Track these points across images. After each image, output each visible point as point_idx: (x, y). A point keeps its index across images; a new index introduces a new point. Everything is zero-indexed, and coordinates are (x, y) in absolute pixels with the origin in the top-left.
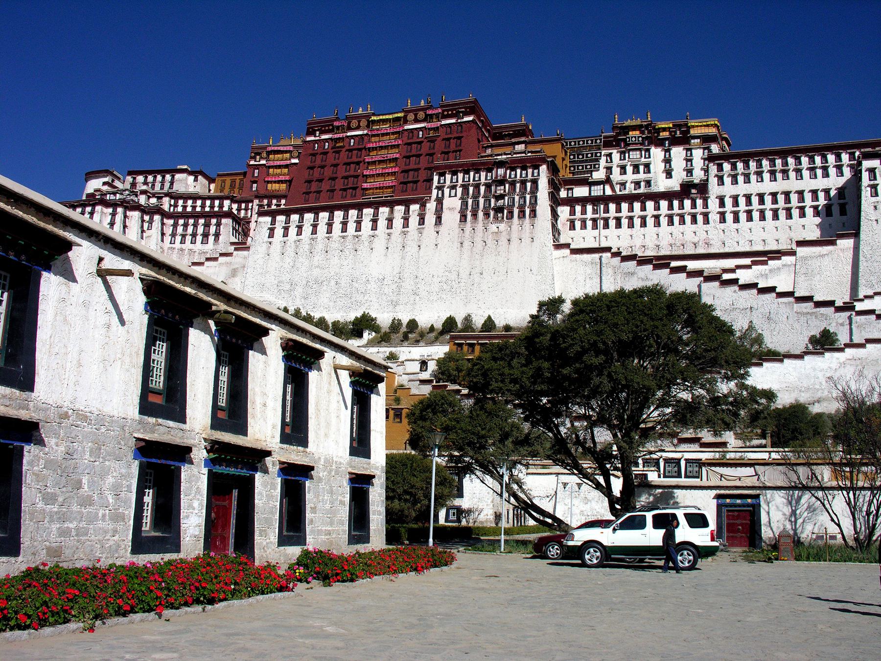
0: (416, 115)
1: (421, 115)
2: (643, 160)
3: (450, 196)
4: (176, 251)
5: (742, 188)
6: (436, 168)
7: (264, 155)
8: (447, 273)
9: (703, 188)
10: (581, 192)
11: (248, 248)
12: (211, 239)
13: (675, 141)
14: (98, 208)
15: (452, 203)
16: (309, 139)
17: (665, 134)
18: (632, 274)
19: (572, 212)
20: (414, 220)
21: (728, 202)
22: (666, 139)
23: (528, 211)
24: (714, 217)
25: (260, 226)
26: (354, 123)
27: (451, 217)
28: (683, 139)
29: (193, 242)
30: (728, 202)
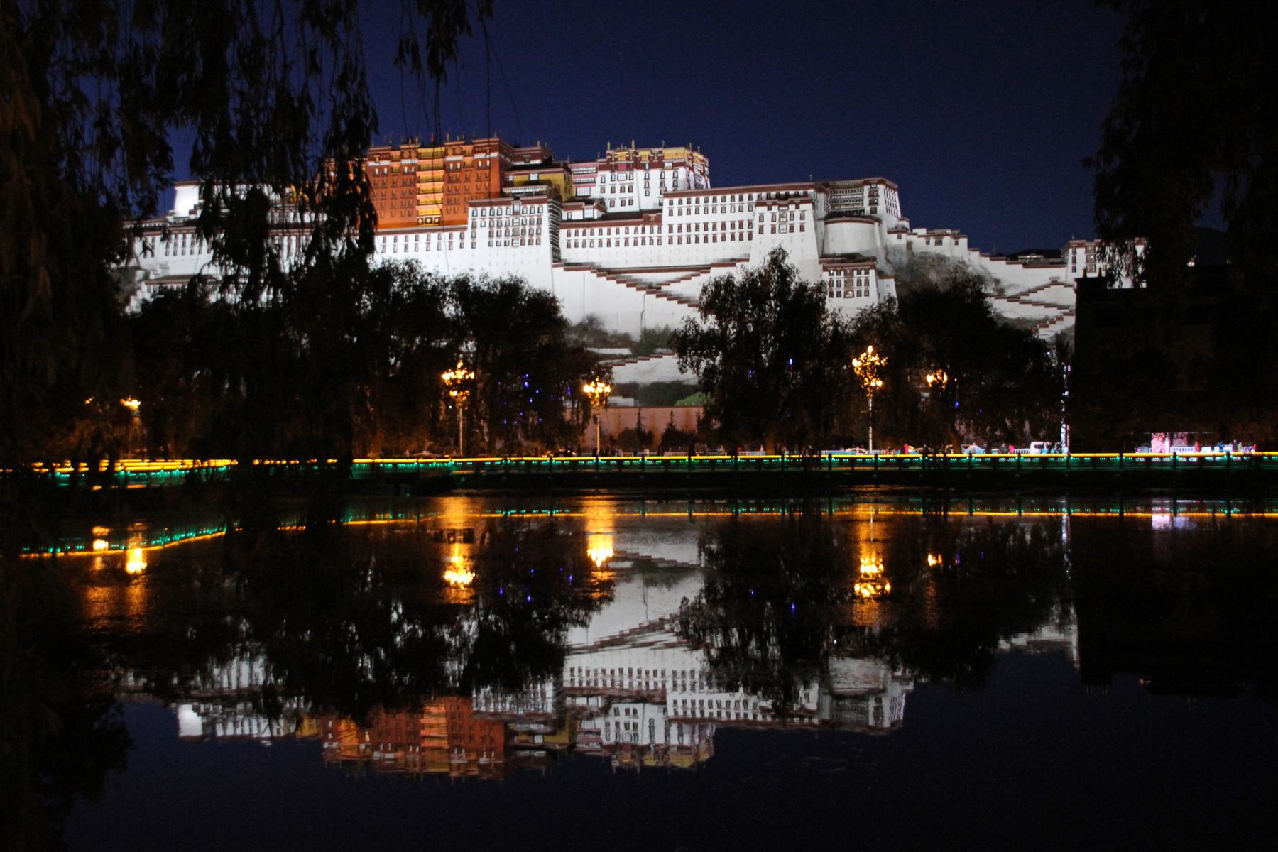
1: (458, 151)
5: (685, 219)
6: (473, 205)
9: (659, 221)
10: (577, 215)
13: (653, 166)
15: (482, 233)
17: (645, 161)
19: (569, 235)
21: (675, 229)
23: (535, 238)
24: (665, 240)
26: (406, 154)
28: (658, 164)
30: (675, 229)
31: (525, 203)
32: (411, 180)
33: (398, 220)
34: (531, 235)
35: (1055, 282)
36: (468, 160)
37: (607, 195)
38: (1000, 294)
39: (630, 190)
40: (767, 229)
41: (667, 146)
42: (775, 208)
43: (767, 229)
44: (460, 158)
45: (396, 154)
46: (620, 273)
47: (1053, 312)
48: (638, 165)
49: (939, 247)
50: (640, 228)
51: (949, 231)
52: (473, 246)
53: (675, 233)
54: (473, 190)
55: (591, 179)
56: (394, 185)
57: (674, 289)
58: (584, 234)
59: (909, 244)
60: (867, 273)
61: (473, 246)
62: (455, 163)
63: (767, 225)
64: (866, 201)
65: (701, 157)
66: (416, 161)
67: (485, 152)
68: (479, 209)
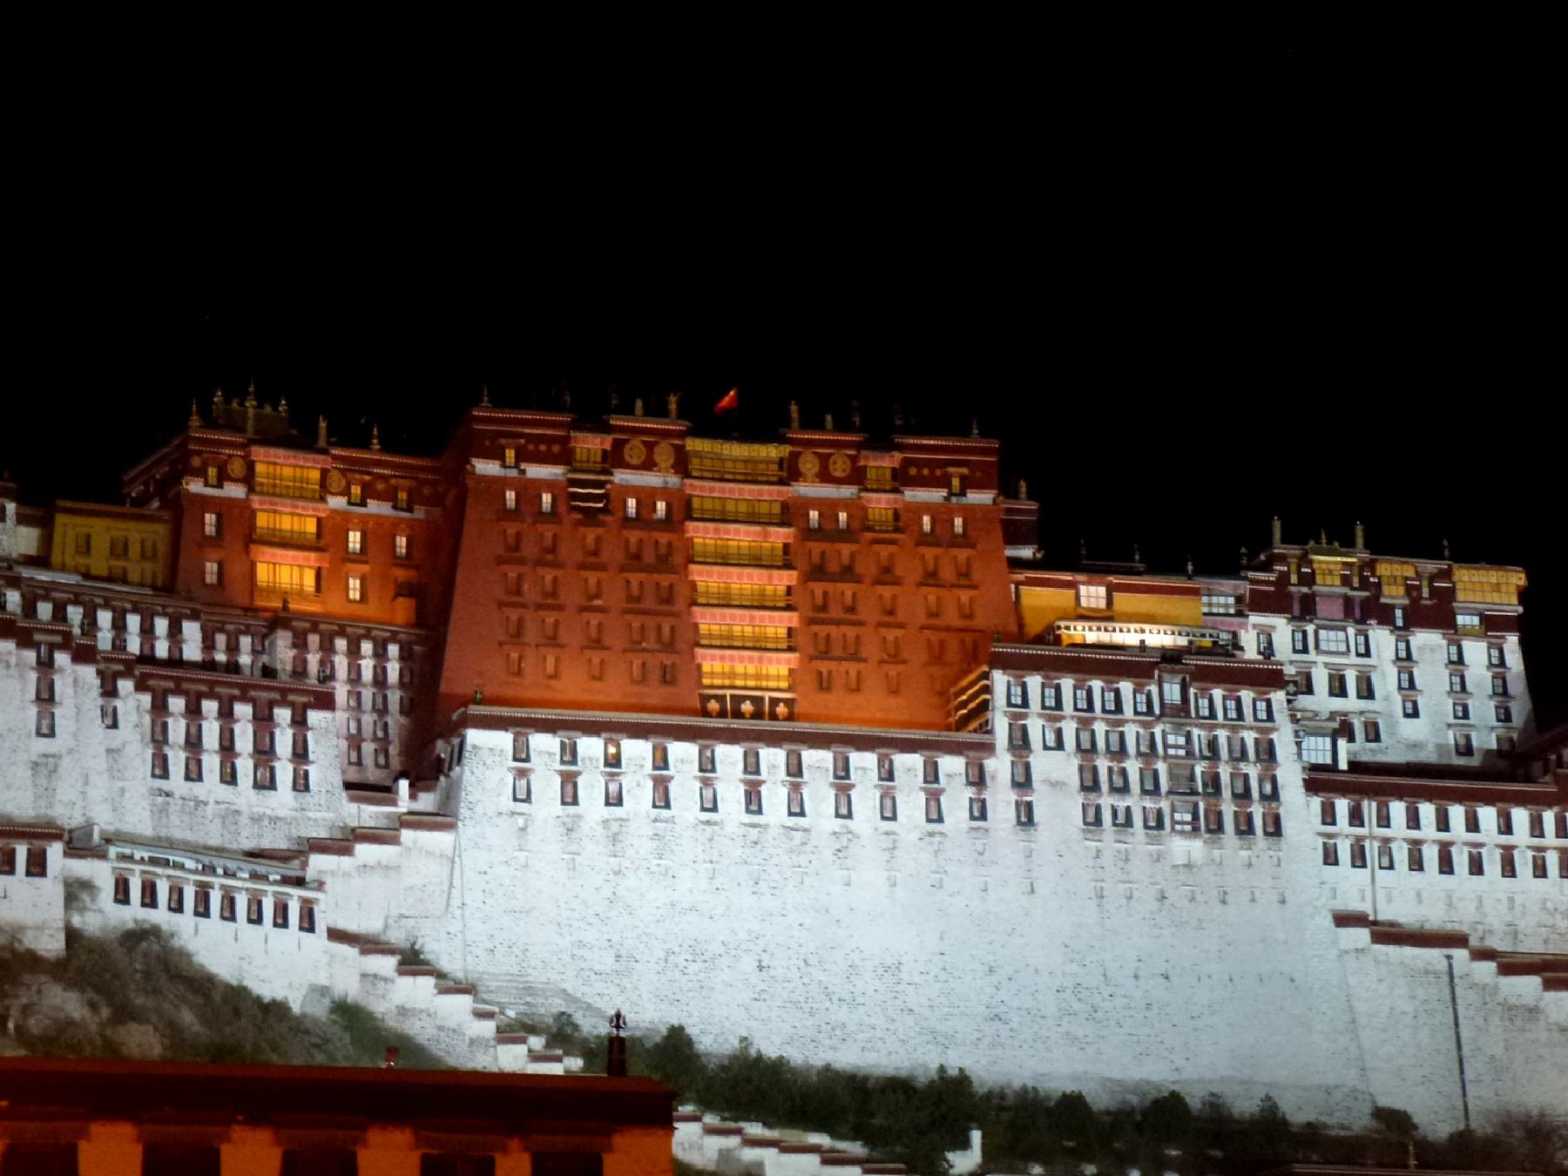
0: (824, 460)
2: (1353, 659)
3: (1046, 748)
4: (175, 805)
7: (237, 468)
8: (1074, 967)
12: (284, 771)
13: (1419, 617)
15: (1055, 769)
16: (486, 467)
17: (1394, 595)
18: (1533, 1011)
20: (956, 800)
22: (1392, 608)
26: (635, 450)
27: (1060, 807)
28: (1435, 612)
29: (229, 777)
34: (1243, 796)
36: (880, 504)
39: (1367, 692)
44: (847, 491)
45: (591, 444)
48: (1367, 610)
52: (1026, 817)
56: (592, 560)
58: (1356, 817)
61: (1026, 817)
62: (829, 508)
66: (674, 480)
67: (944, 482)
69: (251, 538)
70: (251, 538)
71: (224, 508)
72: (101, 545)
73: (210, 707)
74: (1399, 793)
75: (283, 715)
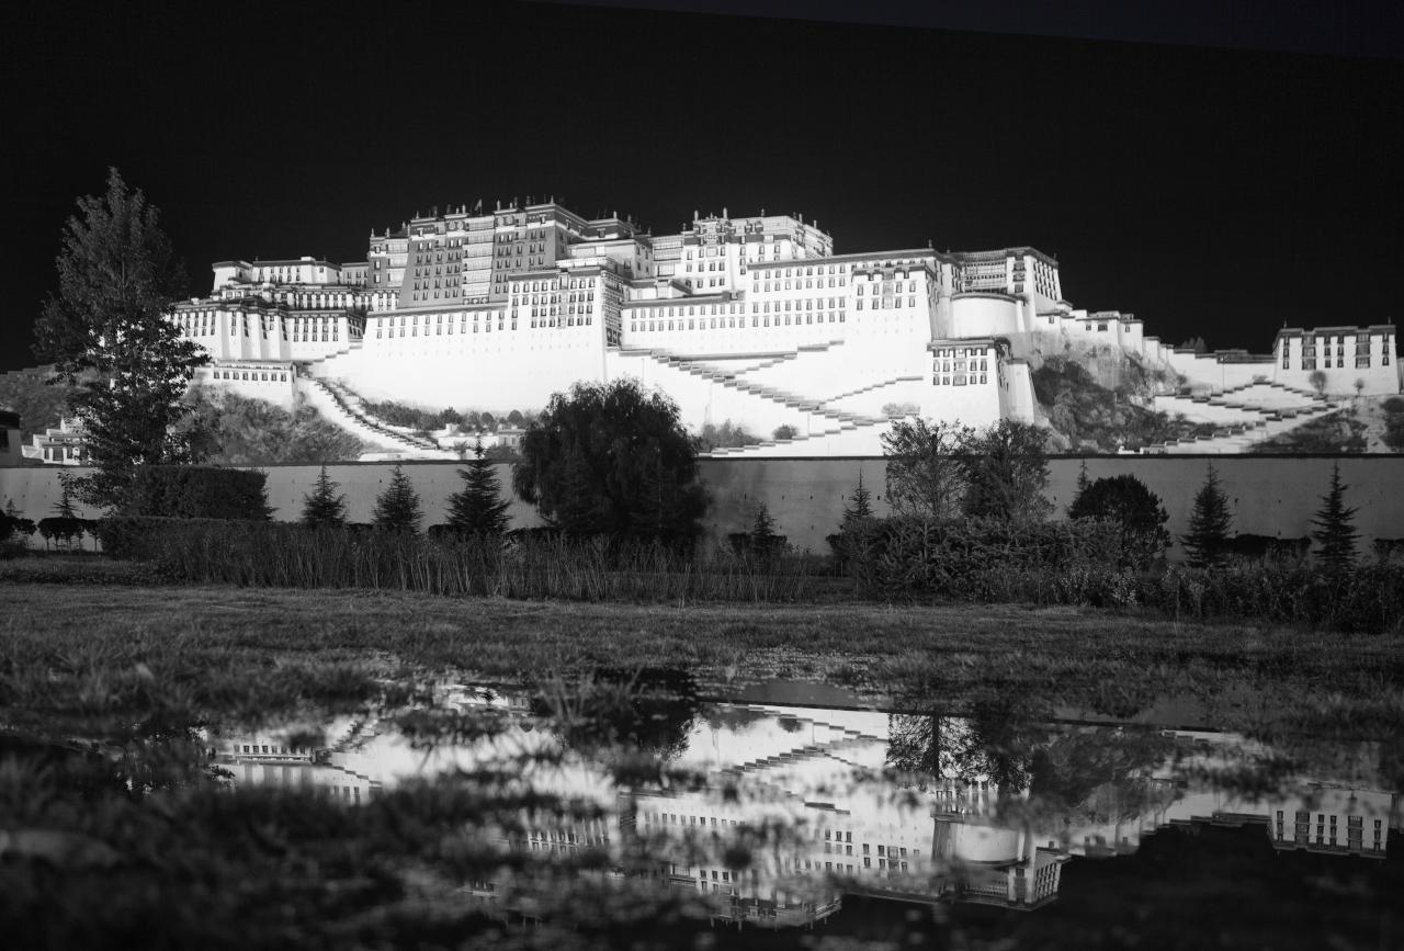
5: (773, 296)
7: (384, 247)
9: (740, 295)
10: (648, 294)
11: (360, 347)
13: (749, 239)
14: (219, 313)
15: (525, 312)
17: (740, 233)
19: (634, 316)
21: (761, 308)
25: (371, 323)
29: (315, 339)
30: (761, 308)
31: (574, 275)
32: (456, 253)
33: (442, 302)
35: (1260, 381)
37: (694, 275)
38: (1185, 393)
39: (721, 268)
40: (868, 304)
41: (766, 215)
42: (878, 278)
43: (868, 304)
46: (691, 360)
47: (1255, 417)
48: (730, 238)
49: (1103, 333)
50: (718, 307)
51: (1117, 314)
53: (761, 314)
54: (525, 264)
55: (676, 256)
57: (752, 378)
59: (1063, 330)
60: (984, 353)
62: (507, 235)
63: (868, 299)
64: (1010, 276)
65: (819, 233)
68: (521, 284)
69: (389, 265)
70: (389, 265)
71: (381, 259)
72: (354, 276)
73: (311, 320)
74: (708, 302)
75: (331, 320)
